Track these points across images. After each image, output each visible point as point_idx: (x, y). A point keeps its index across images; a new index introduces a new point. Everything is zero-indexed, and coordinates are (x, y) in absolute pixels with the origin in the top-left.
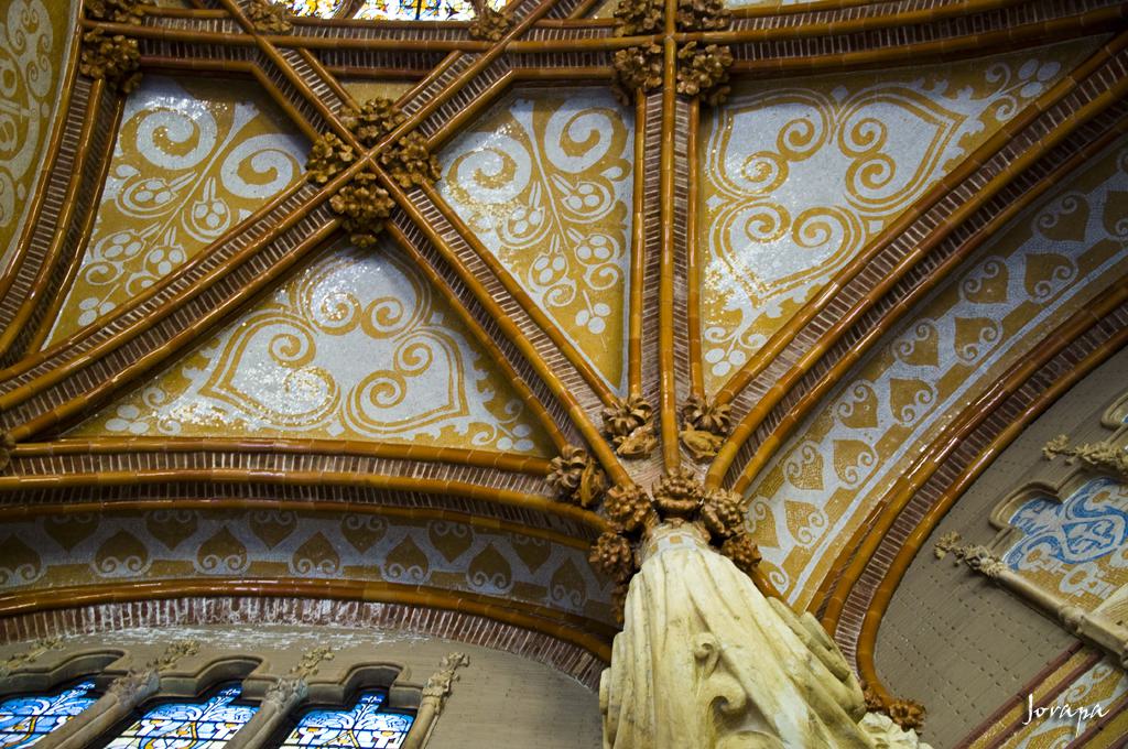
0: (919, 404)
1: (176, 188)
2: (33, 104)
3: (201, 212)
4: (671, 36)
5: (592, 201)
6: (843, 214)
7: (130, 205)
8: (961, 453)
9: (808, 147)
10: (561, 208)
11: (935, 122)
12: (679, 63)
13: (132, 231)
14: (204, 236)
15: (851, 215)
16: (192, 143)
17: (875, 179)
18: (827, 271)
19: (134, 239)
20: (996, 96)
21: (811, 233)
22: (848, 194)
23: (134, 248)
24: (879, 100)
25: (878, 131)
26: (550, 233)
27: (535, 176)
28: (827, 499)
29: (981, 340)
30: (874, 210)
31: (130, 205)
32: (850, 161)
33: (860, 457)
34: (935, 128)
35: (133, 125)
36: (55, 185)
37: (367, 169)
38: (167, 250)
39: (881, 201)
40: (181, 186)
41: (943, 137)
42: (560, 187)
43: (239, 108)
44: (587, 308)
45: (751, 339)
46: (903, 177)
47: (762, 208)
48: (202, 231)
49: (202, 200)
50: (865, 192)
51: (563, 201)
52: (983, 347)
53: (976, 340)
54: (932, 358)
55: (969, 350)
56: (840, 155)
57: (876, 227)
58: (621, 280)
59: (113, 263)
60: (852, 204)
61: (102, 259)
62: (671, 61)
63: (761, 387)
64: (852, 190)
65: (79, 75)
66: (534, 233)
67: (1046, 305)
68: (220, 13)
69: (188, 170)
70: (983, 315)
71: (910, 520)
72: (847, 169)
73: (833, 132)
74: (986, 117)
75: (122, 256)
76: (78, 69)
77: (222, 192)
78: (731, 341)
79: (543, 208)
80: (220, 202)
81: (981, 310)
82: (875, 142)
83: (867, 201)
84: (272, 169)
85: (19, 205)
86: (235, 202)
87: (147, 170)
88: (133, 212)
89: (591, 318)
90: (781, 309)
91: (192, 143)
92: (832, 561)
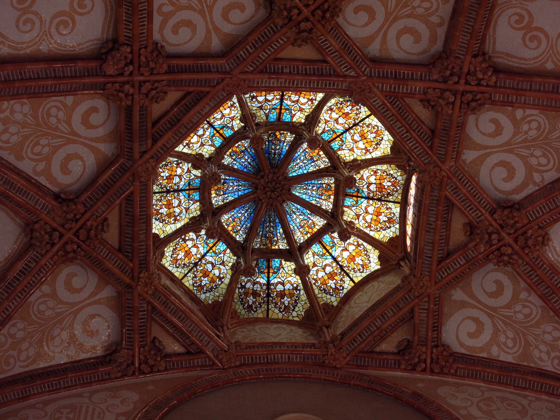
1: (504, 328)
2: (487, 395)
3: (520, 317)
4: (461, 87)
5: (534, 125)
7: (515, 349)
9: (527, 17)
10: (534, 140)
12: (479, 85)
13: (531, 348)
14: (536, 315)
16: (476, 320)
19: (537, 347)
23: (543, 348)
26: (551, 147)
27: (511, 151)
31: (515, 349)
35: (467, 348)
36: (518, 384)
37: (516, 241)
38: (544, 332)
40: (503, 325)
42: (520, 140)
43: (453, 298)
48: (533, 316)
49: (512, 316)
51: (529, 138)
59: (551, 358)
61: (549, 363)
62: (475, 88)
65: (455, 375)
66: (548, 154)
68: (416, 309)
69: (493, 322)
73: (522, 4)
75: (548, 353)
76: (452, 375)
77: (508, 306)
79: (532, 149)
80: (514, 307)
84: (494, 282)
85: (537, 399)
86: (515, 299)
87: (494, 340)
88: (520, 347)
91: (476, 320)
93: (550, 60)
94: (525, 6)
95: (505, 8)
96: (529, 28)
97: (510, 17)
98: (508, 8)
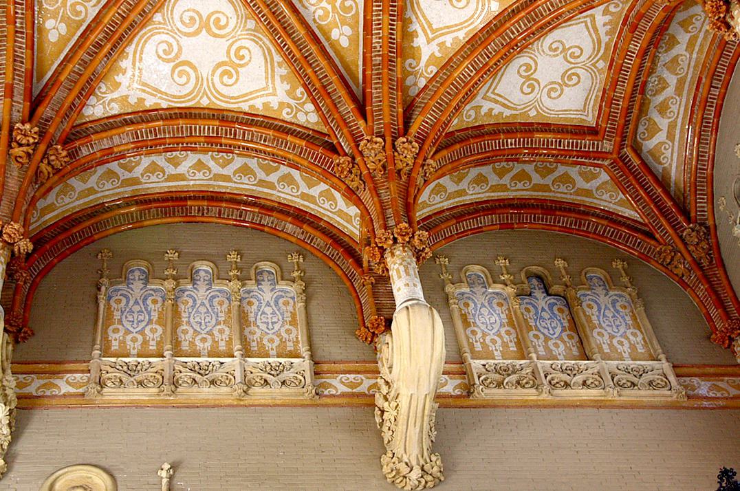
0: (155, 176)
6: (200, 79)
8: (149, 212)
9: (217, 31)
11: (267, 83)
15: (202, 84)
17: (225, 79)
18: (170, 101)
20: (292, 102)
21: (181, 74)
22: (210, 73)
24: (261, 46)
25: (247, 59)
28: (83, 188)
29: (201, 173)
30: (211, 93)
32: (225, 59)
33: (113, 180)
34: (265, 85)
39: (218, 92)
41: (263, 93)
44: (57, 21)
45: (114, 105)
46: (234, 91)
47: (173, 40)
50: (217, 79)
52: (199, 175)
53: (199, 172)
54: (176, 165)
55: (193, 172)
56: (224, 52)
57: (205, 102)
58: (83, 21)
60: (207, 79)
63: (92, 148)
64: (214, 72)
67: (235, 182)
70: (210, 166)
71: (105, 224)
72: (221, 61)
74: (281, 104)
78: (103, 98)
81: (212, 164)
82: (242, 62)
83: (213, 85)
89: (54, 28)
90: (136, 101)
92: (62, 217)
93: (162, 21)
94: (228, 38)
95: (239, 21)
96: (205, 25)
97: (227, 18)
98: (237, 23)
